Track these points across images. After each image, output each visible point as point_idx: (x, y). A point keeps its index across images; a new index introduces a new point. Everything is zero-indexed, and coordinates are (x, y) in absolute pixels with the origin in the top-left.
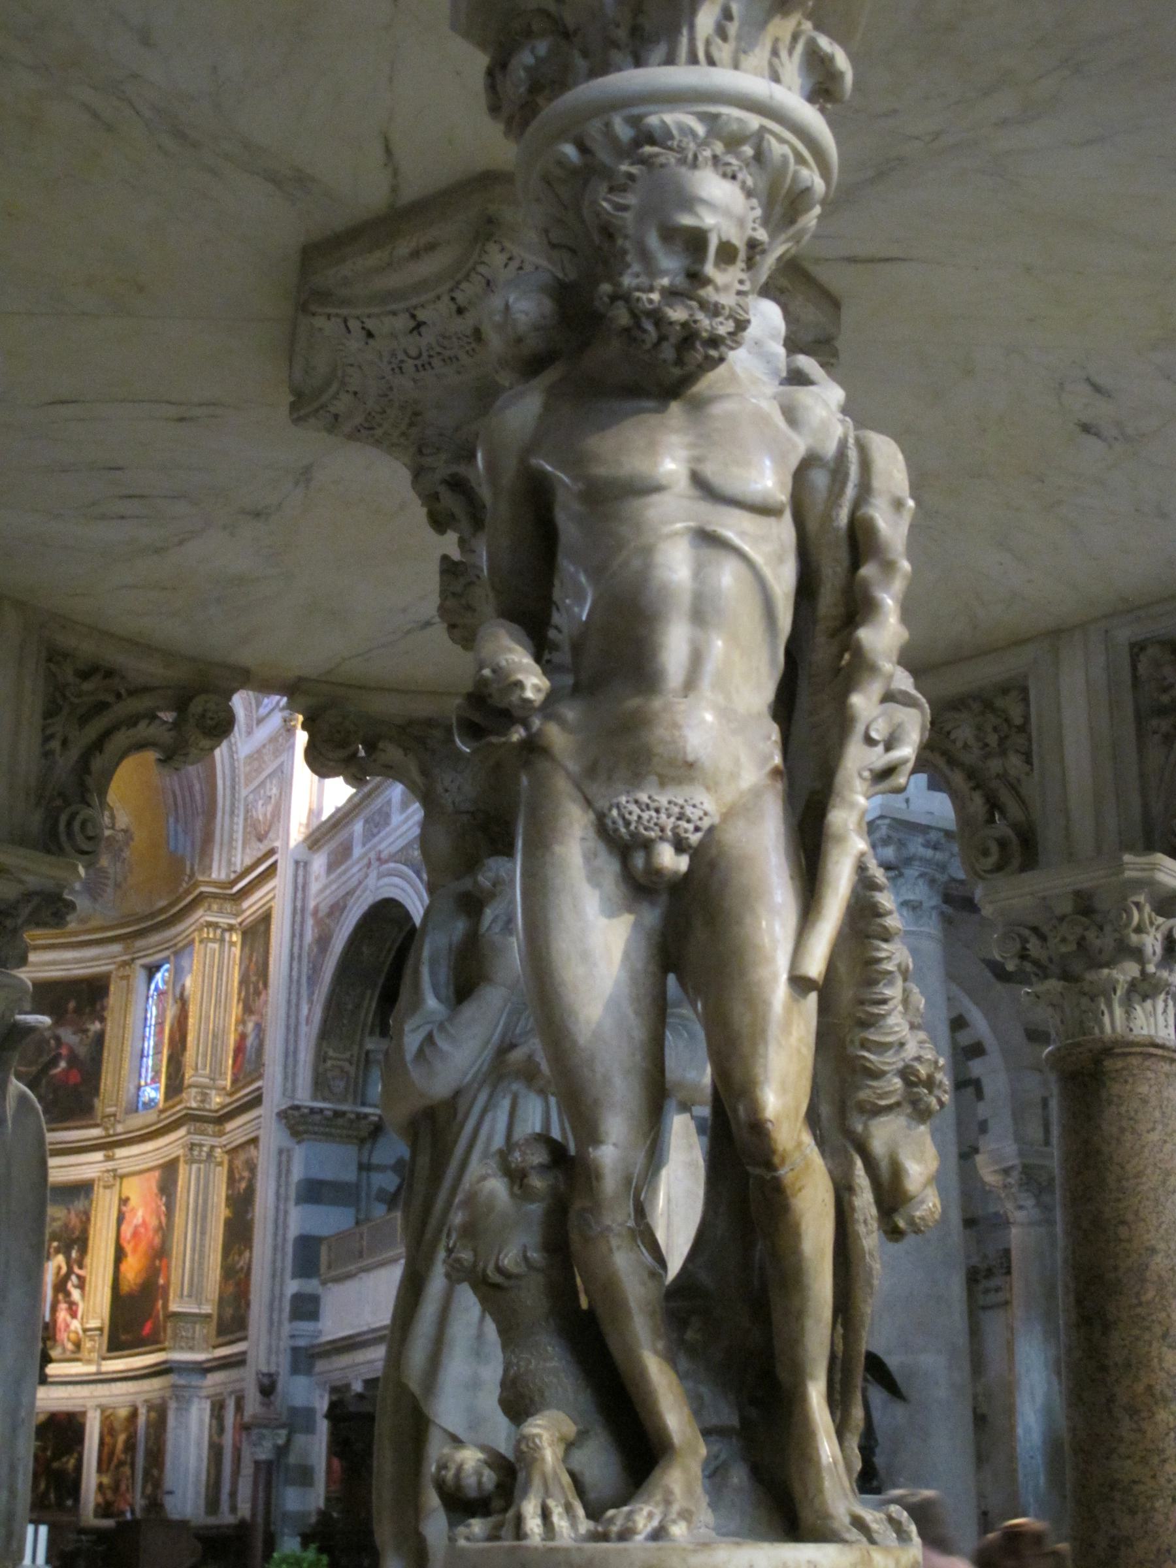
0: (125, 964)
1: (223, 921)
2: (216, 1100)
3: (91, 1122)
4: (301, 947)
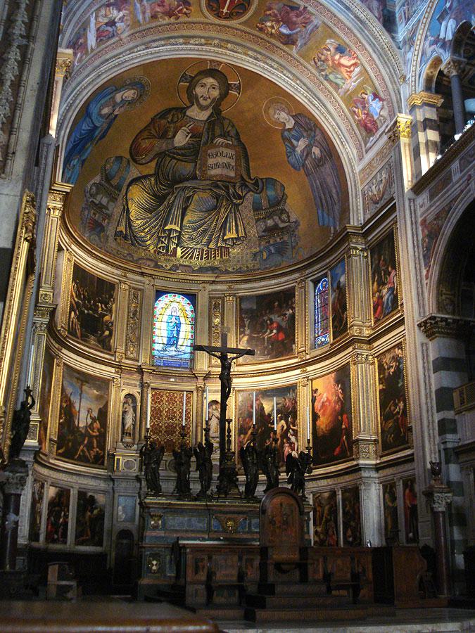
0: (302, 281)
1: (359, 247)
2: (367, 332)
3: (292, 356)
4: (417, 240)
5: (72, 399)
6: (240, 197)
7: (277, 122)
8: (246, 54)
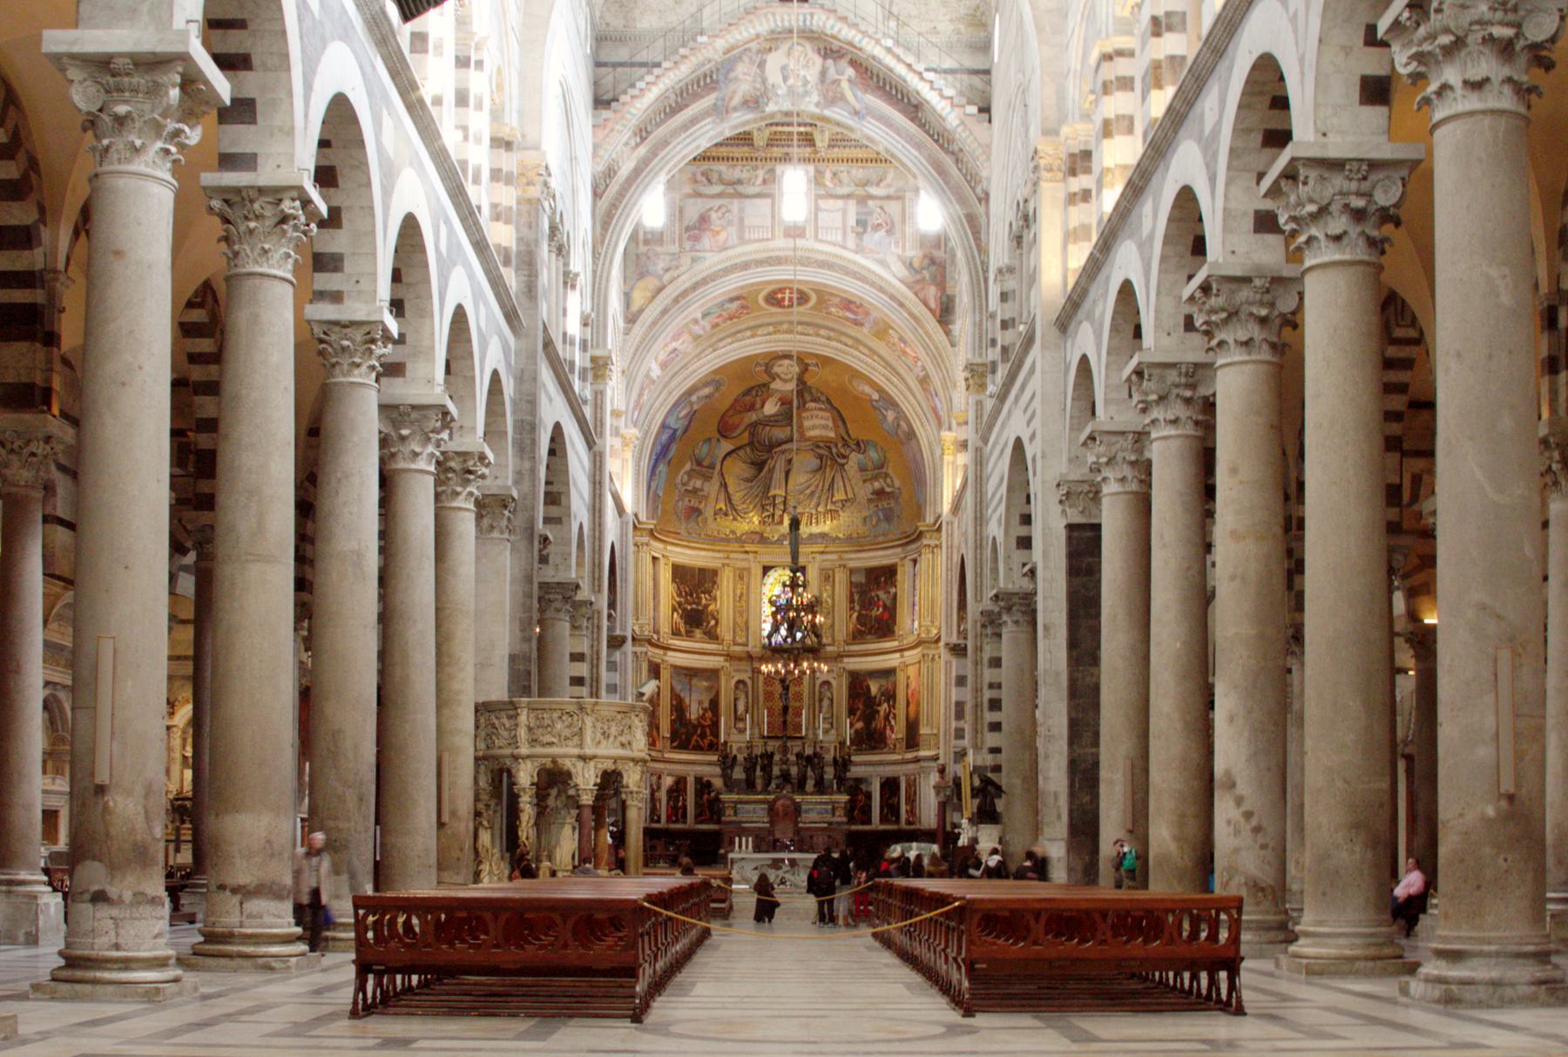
0: (902, 559)
1: (933, 543)
5: (682, 695)
6: (844, 457)
7: (863, 393)
8: (818, 335)
